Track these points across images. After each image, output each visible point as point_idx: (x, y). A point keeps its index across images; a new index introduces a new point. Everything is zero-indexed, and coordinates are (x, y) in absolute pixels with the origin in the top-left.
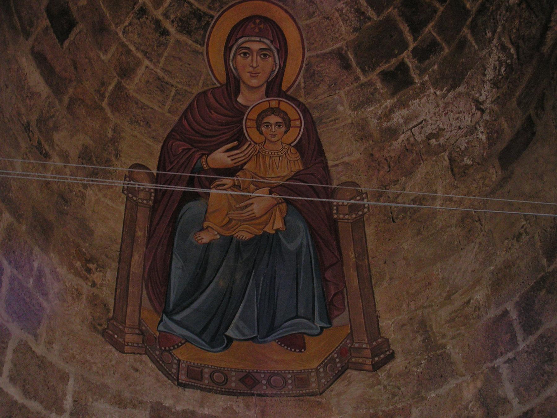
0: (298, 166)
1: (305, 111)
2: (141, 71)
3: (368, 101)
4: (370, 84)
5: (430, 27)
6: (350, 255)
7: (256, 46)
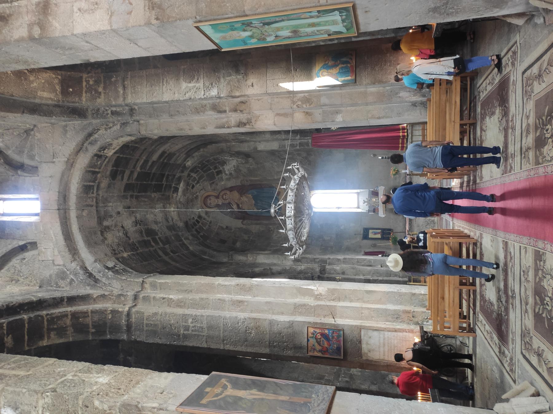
0: (236, 191)
1: (222, 190)
2: (220, 225)
3: (222, 178)
4: (218, 179)
5: (211, 168)
6: (259, 183)
7: (209, 202)
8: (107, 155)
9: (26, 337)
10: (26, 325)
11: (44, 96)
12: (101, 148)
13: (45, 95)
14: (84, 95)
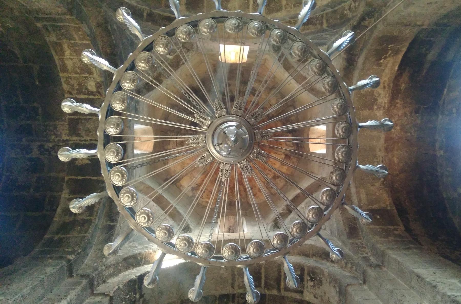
8: (305, 292)
9: (80, 178)
10: (95, 178)
11: (361, 195)
12: (314, 273)
13: (363, 196)
14: (377, 227)
